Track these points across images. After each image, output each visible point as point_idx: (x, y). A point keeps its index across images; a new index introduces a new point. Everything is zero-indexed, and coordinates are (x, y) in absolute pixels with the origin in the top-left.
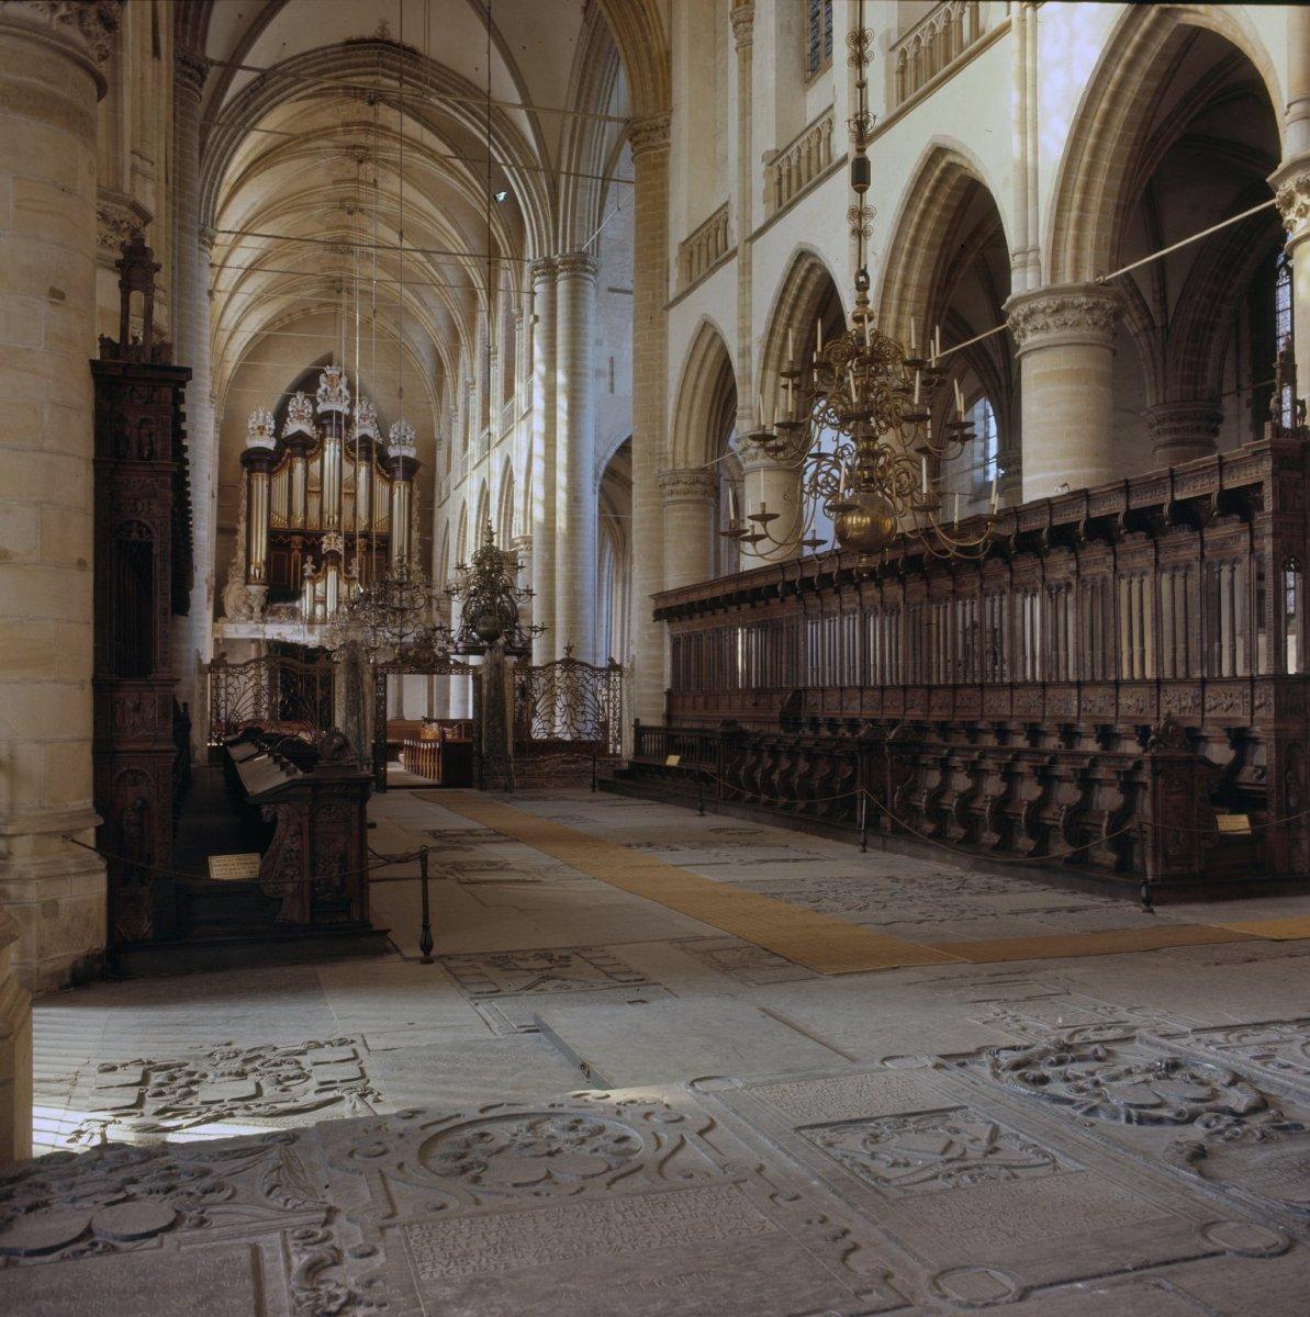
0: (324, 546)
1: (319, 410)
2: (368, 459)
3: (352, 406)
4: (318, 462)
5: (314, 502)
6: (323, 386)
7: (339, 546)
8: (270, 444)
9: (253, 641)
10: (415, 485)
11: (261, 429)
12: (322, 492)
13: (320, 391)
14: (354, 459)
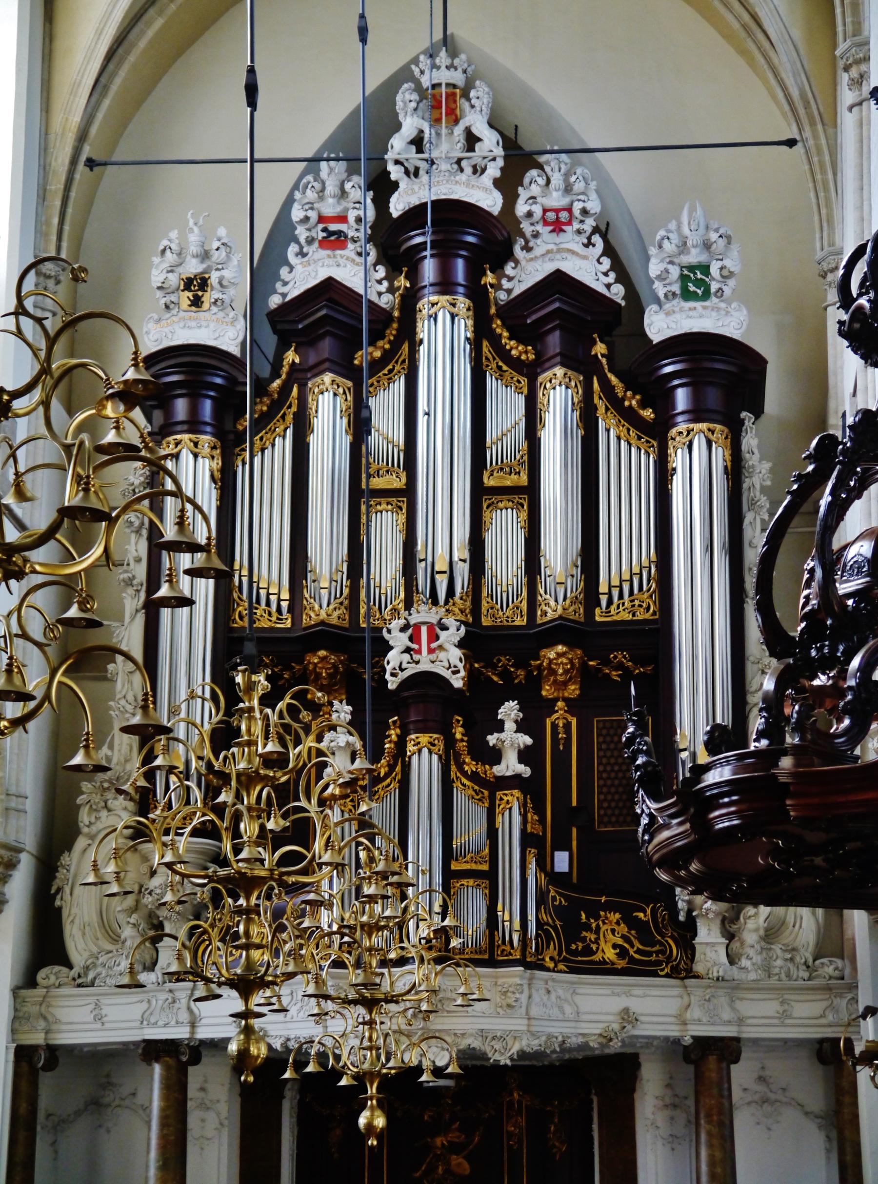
0: (393, 658)
1: (397, 206)
2: (579, 363)
3: (508, 184)
4: (399, 386)
5: (385, 529)
6: (410, 125)
7: (448, 661)
8: (223, 330)
9: (153, 1050)
10: (750, 441)
11: (197, 286)
12: (409, 492)
13: (398, 144)
14: (516, 364)
